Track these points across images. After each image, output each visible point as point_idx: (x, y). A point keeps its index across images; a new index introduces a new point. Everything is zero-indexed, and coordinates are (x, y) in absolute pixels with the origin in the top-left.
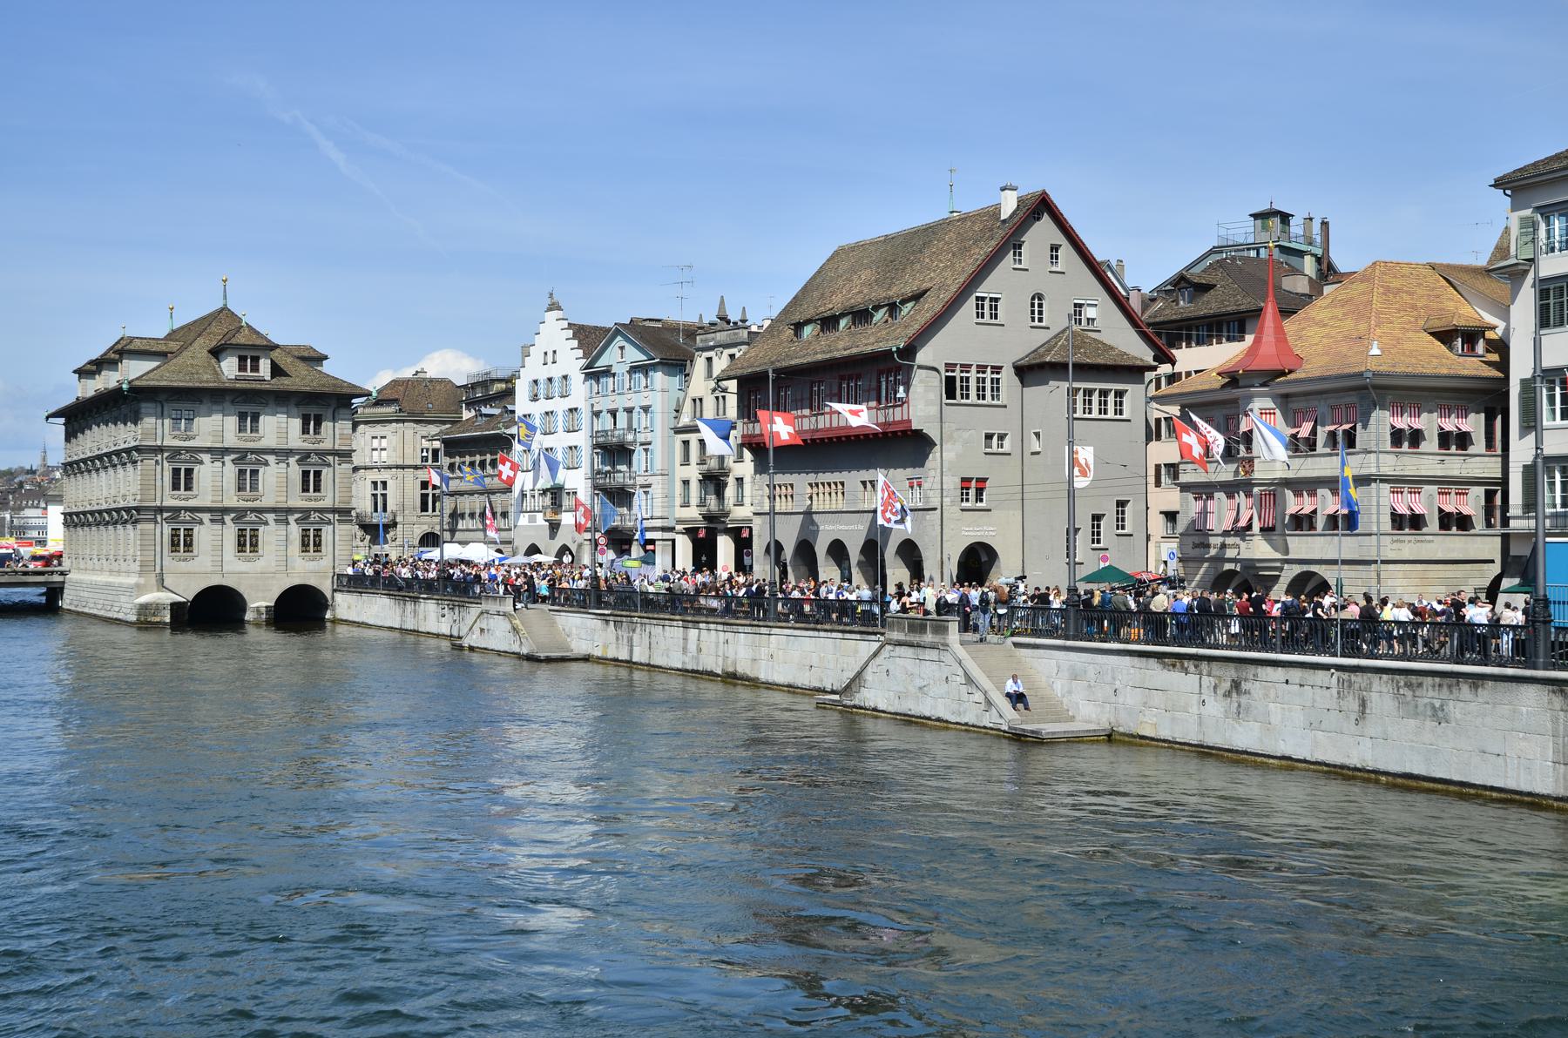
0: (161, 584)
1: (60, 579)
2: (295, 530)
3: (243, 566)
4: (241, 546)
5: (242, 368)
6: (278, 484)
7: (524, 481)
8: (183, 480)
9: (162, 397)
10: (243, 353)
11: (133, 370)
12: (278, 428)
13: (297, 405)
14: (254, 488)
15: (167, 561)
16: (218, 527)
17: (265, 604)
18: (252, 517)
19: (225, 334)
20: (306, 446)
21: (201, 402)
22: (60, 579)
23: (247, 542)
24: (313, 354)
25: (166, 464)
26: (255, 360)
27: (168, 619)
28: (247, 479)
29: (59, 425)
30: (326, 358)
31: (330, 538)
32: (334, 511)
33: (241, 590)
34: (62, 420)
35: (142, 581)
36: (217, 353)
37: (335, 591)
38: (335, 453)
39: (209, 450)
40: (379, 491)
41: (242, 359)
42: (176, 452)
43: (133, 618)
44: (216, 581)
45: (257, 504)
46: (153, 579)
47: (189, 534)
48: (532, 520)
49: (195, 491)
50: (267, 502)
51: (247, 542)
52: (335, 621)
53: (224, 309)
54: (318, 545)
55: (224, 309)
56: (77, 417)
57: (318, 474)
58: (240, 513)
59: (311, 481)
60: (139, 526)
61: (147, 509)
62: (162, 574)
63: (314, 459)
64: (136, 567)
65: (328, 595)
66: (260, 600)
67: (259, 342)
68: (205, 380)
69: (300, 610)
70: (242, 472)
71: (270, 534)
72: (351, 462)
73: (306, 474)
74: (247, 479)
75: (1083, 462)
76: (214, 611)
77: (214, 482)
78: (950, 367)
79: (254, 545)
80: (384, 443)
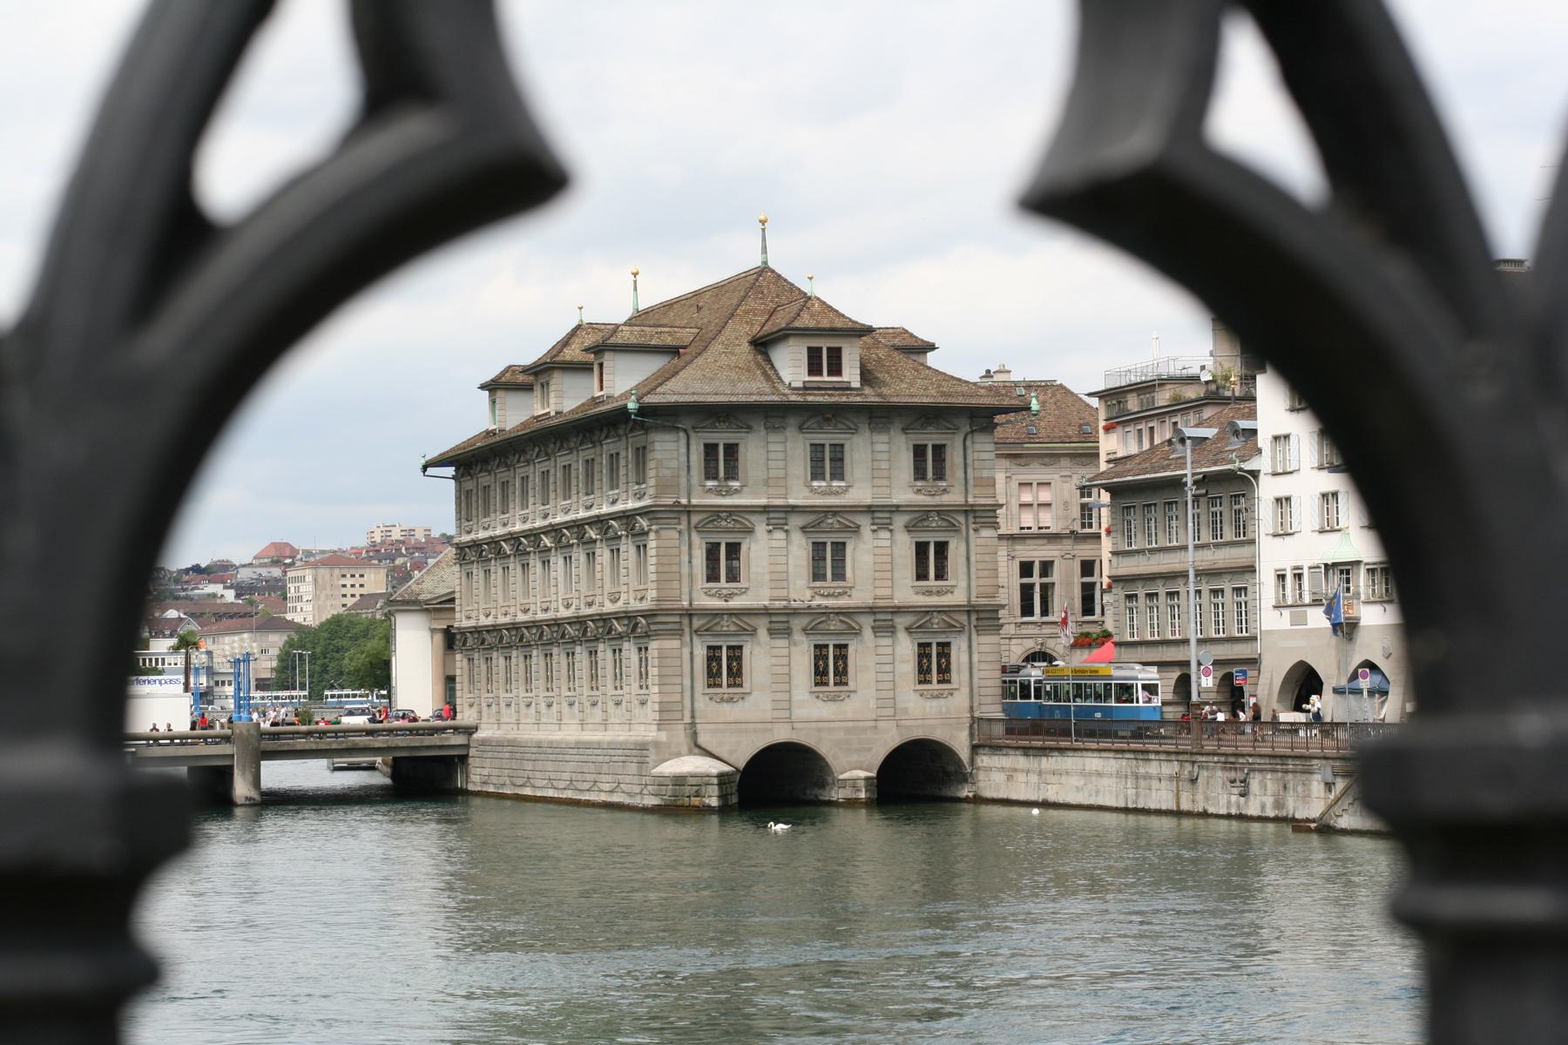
1: (459, 740)
2: (906, 648)
3: (825, 710)
4: (820, 674)
5: (814, 369)
6: (879, 566)
7: (1272, 556)
8: (723, 560)
9: (686, 423)
10: (815, 343)
11: (623, 381)
12: (879, 470)
13: (904, 430)
14: (839, 575)
16: (782, 643)
17: (863, 774)
18: (835, 624)
19: (768, 311)
20: (922, 499)
21: (750, 428)
22: (459, 740)
23: (830, 668)
24: (912, 342)
25: (696, 538)
26: (835, 356)
27: (714, 802)
28: (828, 560)
29: (444, 485)
30: (932, 347)
31: (964, 658)
32: (970, 610)
33: (823, 749)
34: (450, 471)
35: (663, 736)
36: (763, 345)
37: (975, 749)
38: (969, 511)
39: (765, 510)
40: (1036, 579)
41: (814, 356)
42: (716, 513)
43: (651, 801)
44: (782, 735)
45: (843, 602)
46: (681, 736)
47: (736, 653)
48: (1299, 620)
49: (743, 584)
50: (861, 596)
51: (830, 668)
52: (978, 800)
53: (764, 269)
54: (945, 672)
55: (764, 269)
56: (477, 465)
57: (942, 548)
58: (817, 618)
59: (930, 560)
60: (654, 645)
61: (668, 612)
62: (693, 724)
63: (935, 522)
64: (651, 712)
65: (964, 754)
66: (853, 768)
67: (838, 324)
68: (751, 389)
69: (917, 780)
70: (818, 548)
71: (865, 654)
72: (995, 526)
73: (921, 549)
74: (828, 560)
76: (778, 783)
77: (775, 566)
80: (1045, 496)
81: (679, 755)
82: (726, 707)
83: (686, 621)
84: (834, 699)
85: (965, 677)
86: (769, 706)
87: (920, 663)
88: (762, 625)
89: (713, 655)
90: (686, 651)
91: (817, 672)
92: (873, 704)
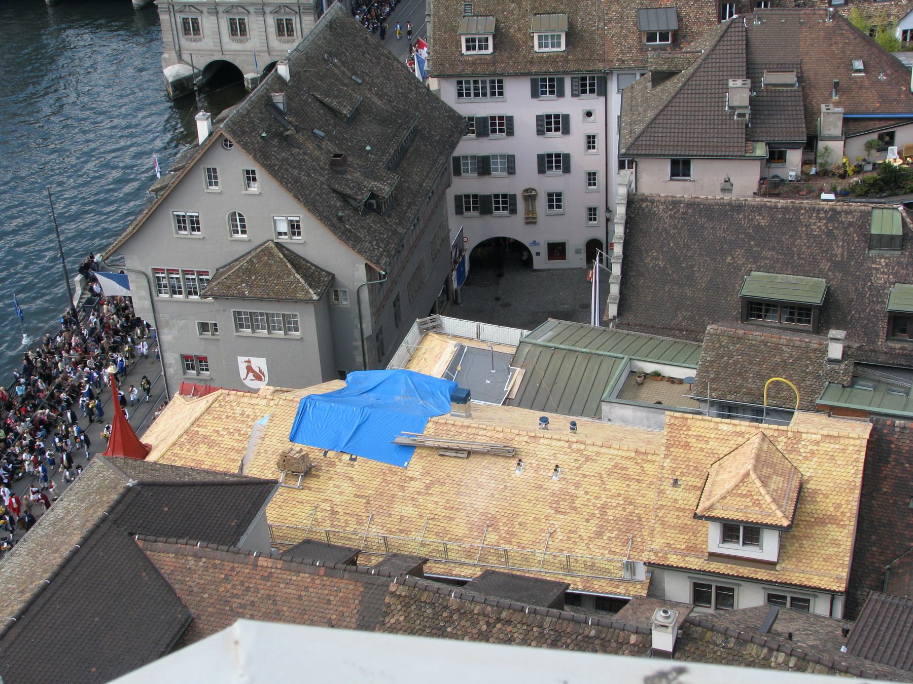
0: (180, 59)
2: (271, 21)
4: (233, 32)
15: (184, 42)
23: (238, 29)
31: (299, 26)
33: (237, 64)
44: (218, 57)
46: (174, 56)
51: (238, 29)
75: (257, 370)
78: (156, 271)
79: (243, 32)
81: (174, 64)
82: (194, 44)
83: (171, 7)
84: (241, 42)
85: (299, 34)
86: (212, 44)
87: (279, 28)
88: (205, 10)
89: (185, 21)
90: (173, 20)
91: (232, 30)
92: (258, 45)
